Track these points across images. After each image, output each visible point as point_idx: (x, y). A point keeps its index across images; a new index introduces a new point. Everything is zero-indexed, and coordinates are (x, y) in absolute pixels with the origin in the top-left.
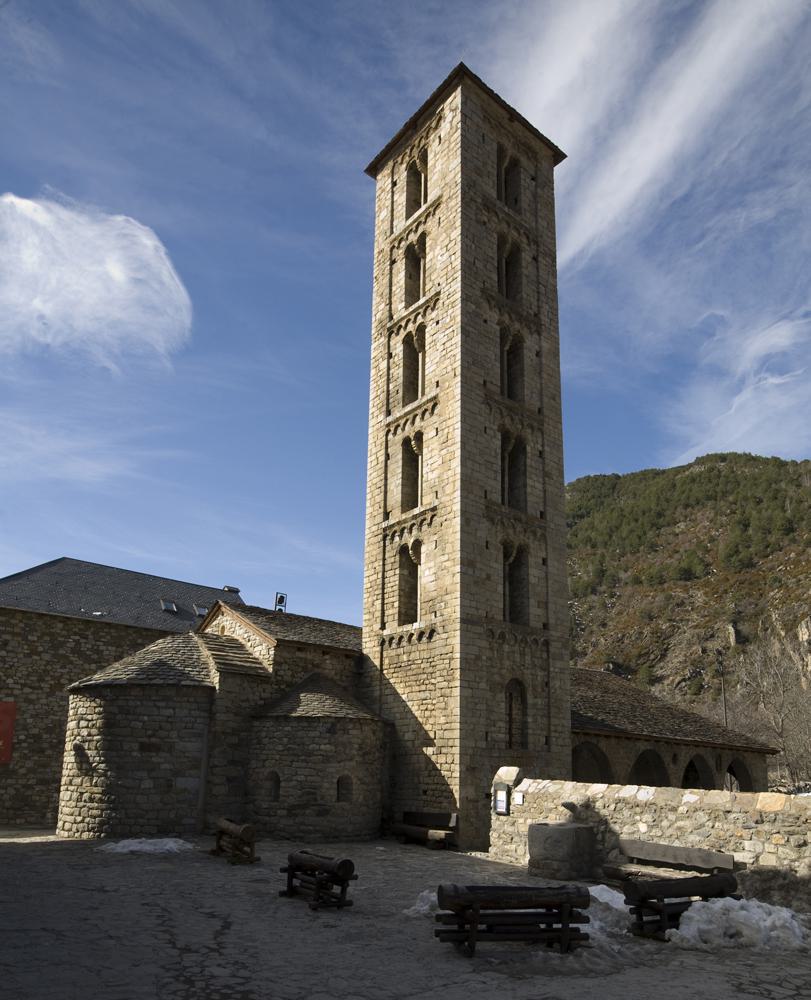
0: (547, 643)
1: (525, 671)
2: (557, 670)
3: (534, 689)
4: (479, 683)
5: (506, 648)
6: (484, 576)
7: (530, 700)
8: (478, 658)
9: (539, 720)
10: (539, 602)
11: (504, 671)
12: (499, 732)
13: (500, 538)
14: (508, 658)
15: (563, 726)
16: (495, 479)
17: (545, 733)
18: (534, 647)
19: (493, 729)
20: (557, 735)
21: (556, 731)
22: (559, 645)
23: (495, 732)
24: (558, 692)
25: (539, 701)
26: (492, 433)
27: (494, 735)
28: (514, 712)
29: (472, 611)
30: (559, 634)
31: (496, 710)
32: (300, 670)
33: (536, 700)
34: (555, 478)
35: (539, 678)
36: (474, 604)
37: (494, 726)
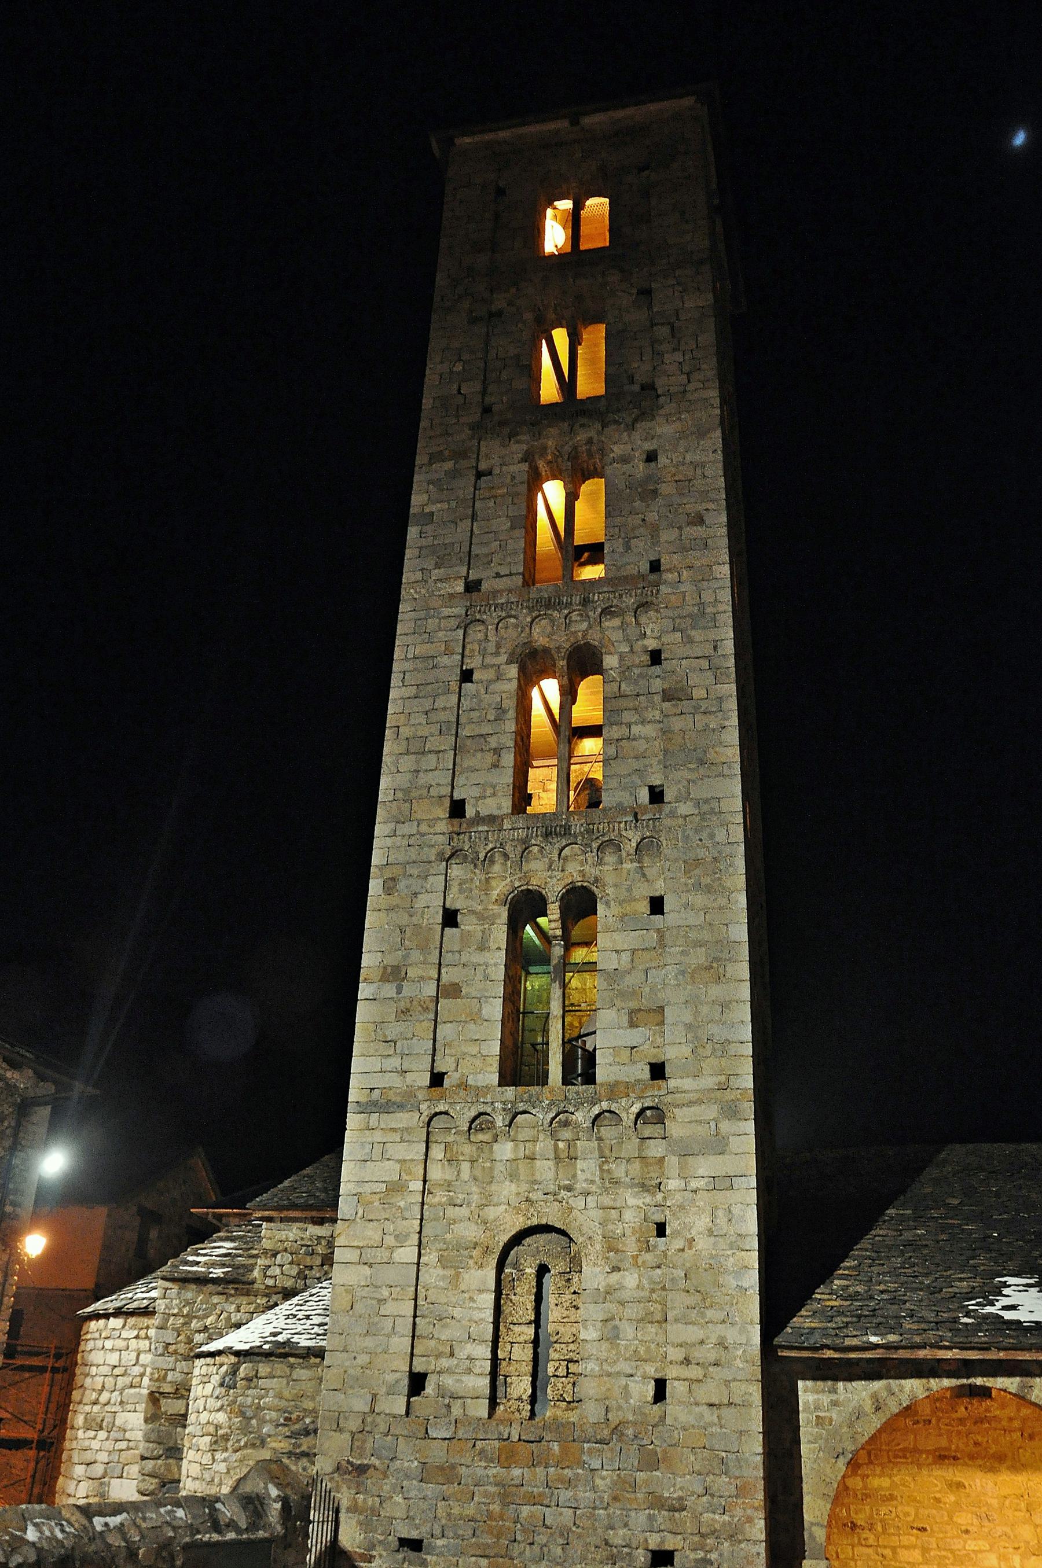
0: (653, 1115)
1: (580, 1203)
2: (694, 1184)
3: (612, 1245)
4: (392, 1249)
5: (505, 1150)
6: (430, 990)
7: (593, 1275)
8: (396, 1188)
9: (628, 1331)
10: (632, 1013)
11: (491, 1213)
12: (469, 1371)
13: (500, 888)
14: (513, 1176)
15: (722, 1344)
16: (495, 766)
17: (651, 1370)
18: (607, 1132)
19: (445, 1363)
20: (695, 1372)
21: (687, 1361)
22: (711, 1112)
23: (449, 1371)
24: (703, 1244)
25: (630, 1280)
26: (491, 674)
27: (448, 1381)
28: (553, 1314)
29: (394, 1081)
30: (709, 1081)
31: (457, 1313)
32: (319, 1262)
33: (615, 1277)
34: (699, 693)
35: (628, 1215)
36: (395, 1062)
37: (452, 1355)
